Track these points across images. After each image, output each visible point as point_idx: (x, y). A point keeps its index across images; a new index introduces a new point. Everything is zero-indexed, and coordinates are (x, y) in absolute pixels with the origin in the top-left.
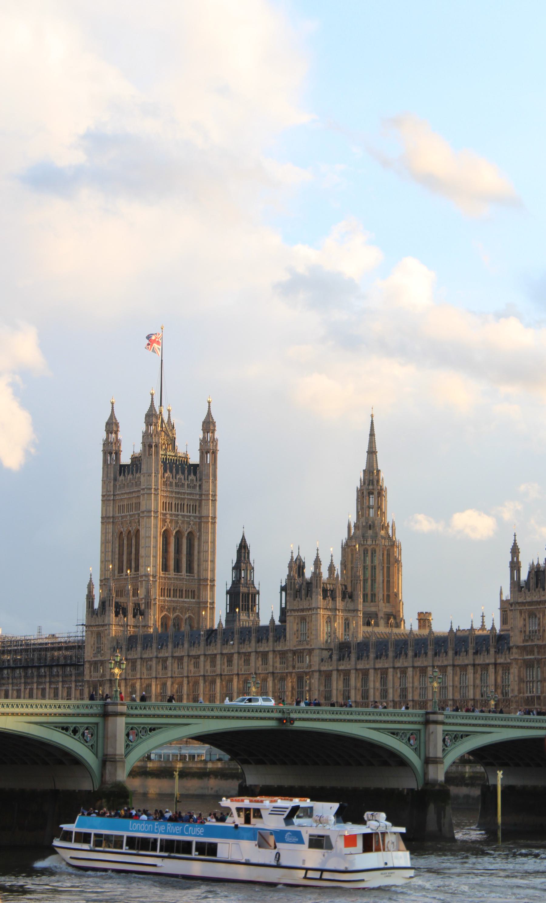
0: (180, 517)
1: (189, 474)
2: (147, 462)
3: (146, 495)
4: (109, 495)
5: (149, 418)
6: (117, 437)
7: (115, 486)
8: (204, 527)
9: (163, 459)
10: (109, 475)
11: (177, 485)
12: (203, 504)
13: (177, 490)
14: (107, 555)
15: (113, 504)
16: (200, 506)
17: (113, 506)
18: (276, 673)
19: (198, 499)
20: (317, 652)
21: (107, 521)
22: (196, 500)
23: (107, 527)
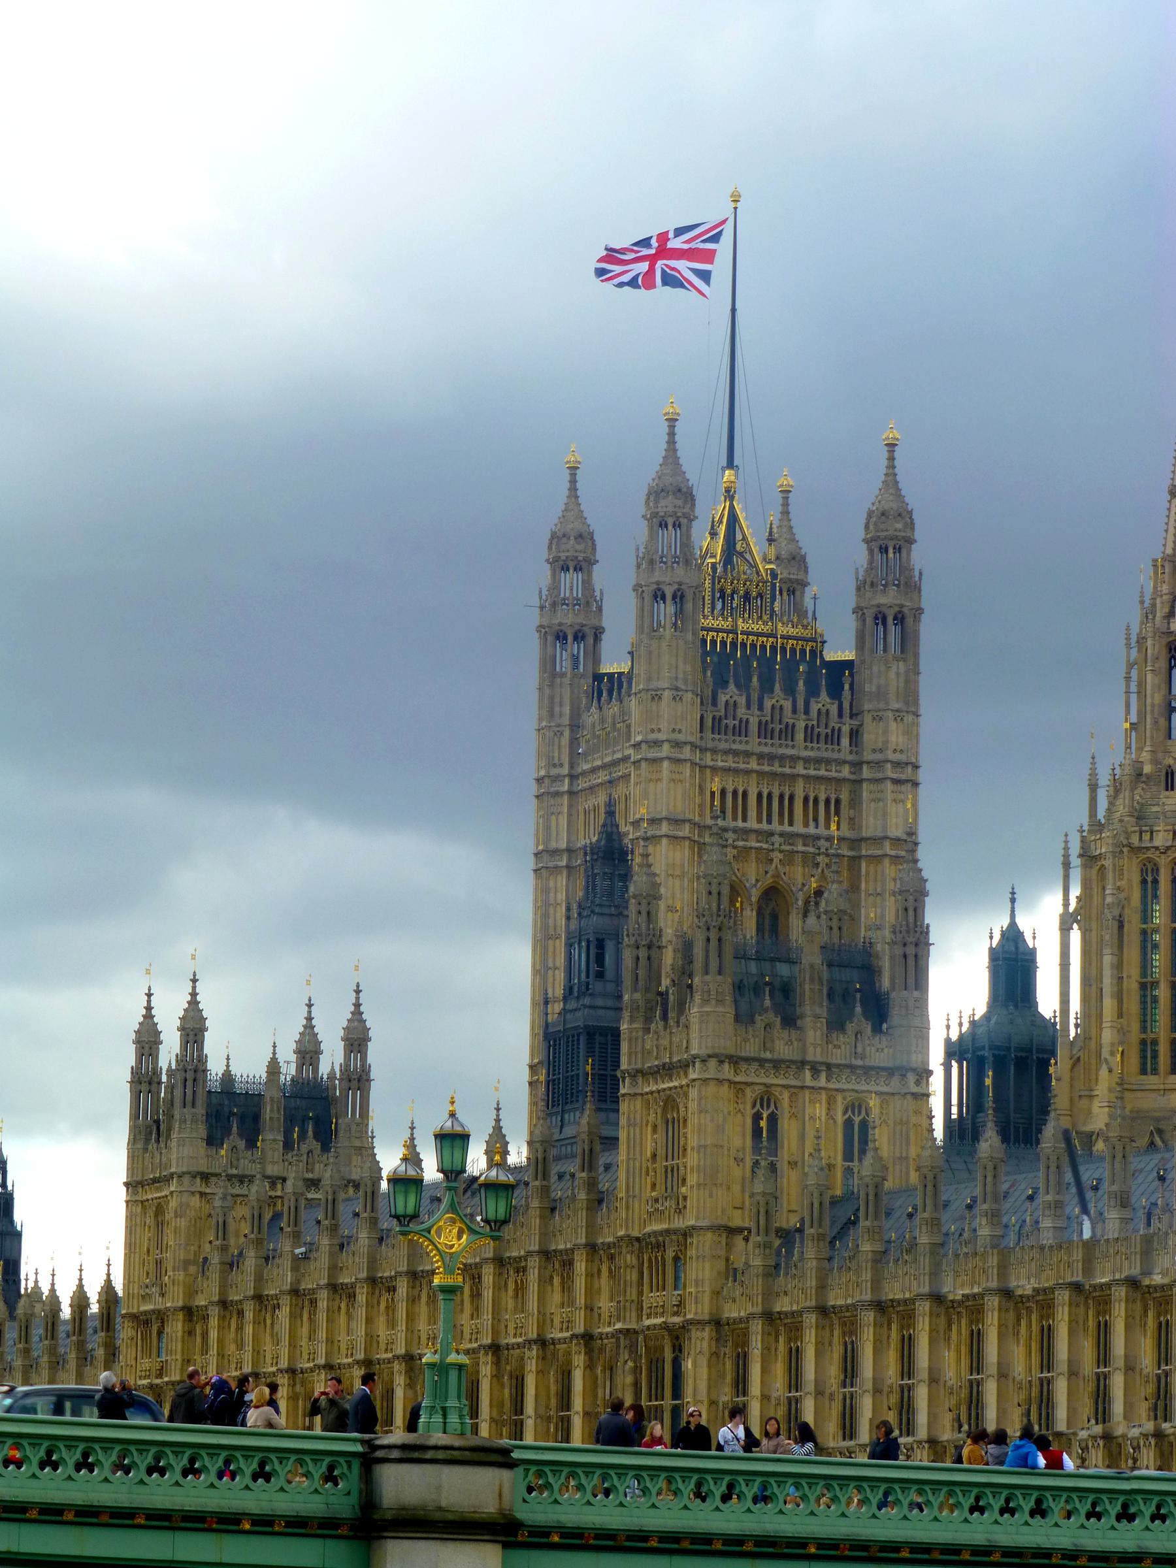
0: (777, 840)
1: (813, 692)
2: (650, 653)
3: (643, 764)
4: (557, 779)
5: (656, 502)
6: (588, 585)
7: (574, 742)
8: (867, 873)
9: (723, 643)
10: (557, 709)
11: (764, 730)
12: (865, 794)
13: (766, 750)
14: (550, 980)
15: (570, 806)
16: (855, 802)
17: (570, 815)
18: (601, 1337)
19: (844, 780)
20: (703, 1245)
21: (551, 864)
22: (839, 781)
23: (552, 884)
